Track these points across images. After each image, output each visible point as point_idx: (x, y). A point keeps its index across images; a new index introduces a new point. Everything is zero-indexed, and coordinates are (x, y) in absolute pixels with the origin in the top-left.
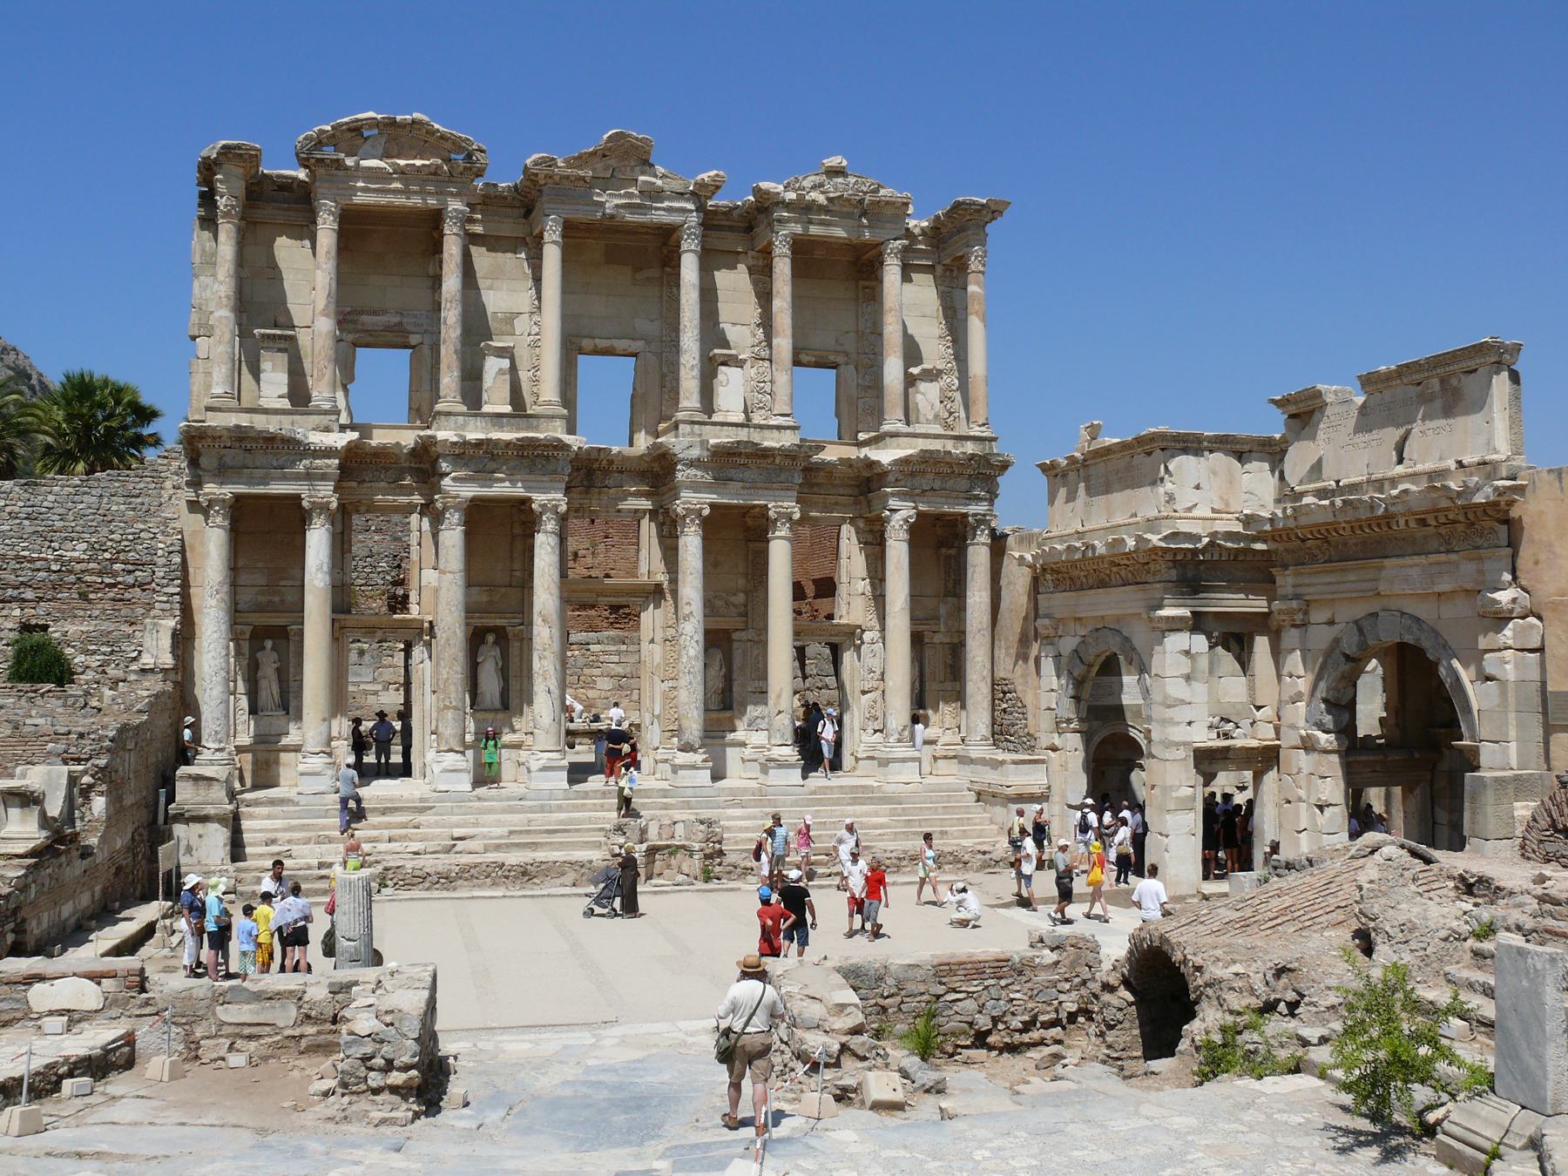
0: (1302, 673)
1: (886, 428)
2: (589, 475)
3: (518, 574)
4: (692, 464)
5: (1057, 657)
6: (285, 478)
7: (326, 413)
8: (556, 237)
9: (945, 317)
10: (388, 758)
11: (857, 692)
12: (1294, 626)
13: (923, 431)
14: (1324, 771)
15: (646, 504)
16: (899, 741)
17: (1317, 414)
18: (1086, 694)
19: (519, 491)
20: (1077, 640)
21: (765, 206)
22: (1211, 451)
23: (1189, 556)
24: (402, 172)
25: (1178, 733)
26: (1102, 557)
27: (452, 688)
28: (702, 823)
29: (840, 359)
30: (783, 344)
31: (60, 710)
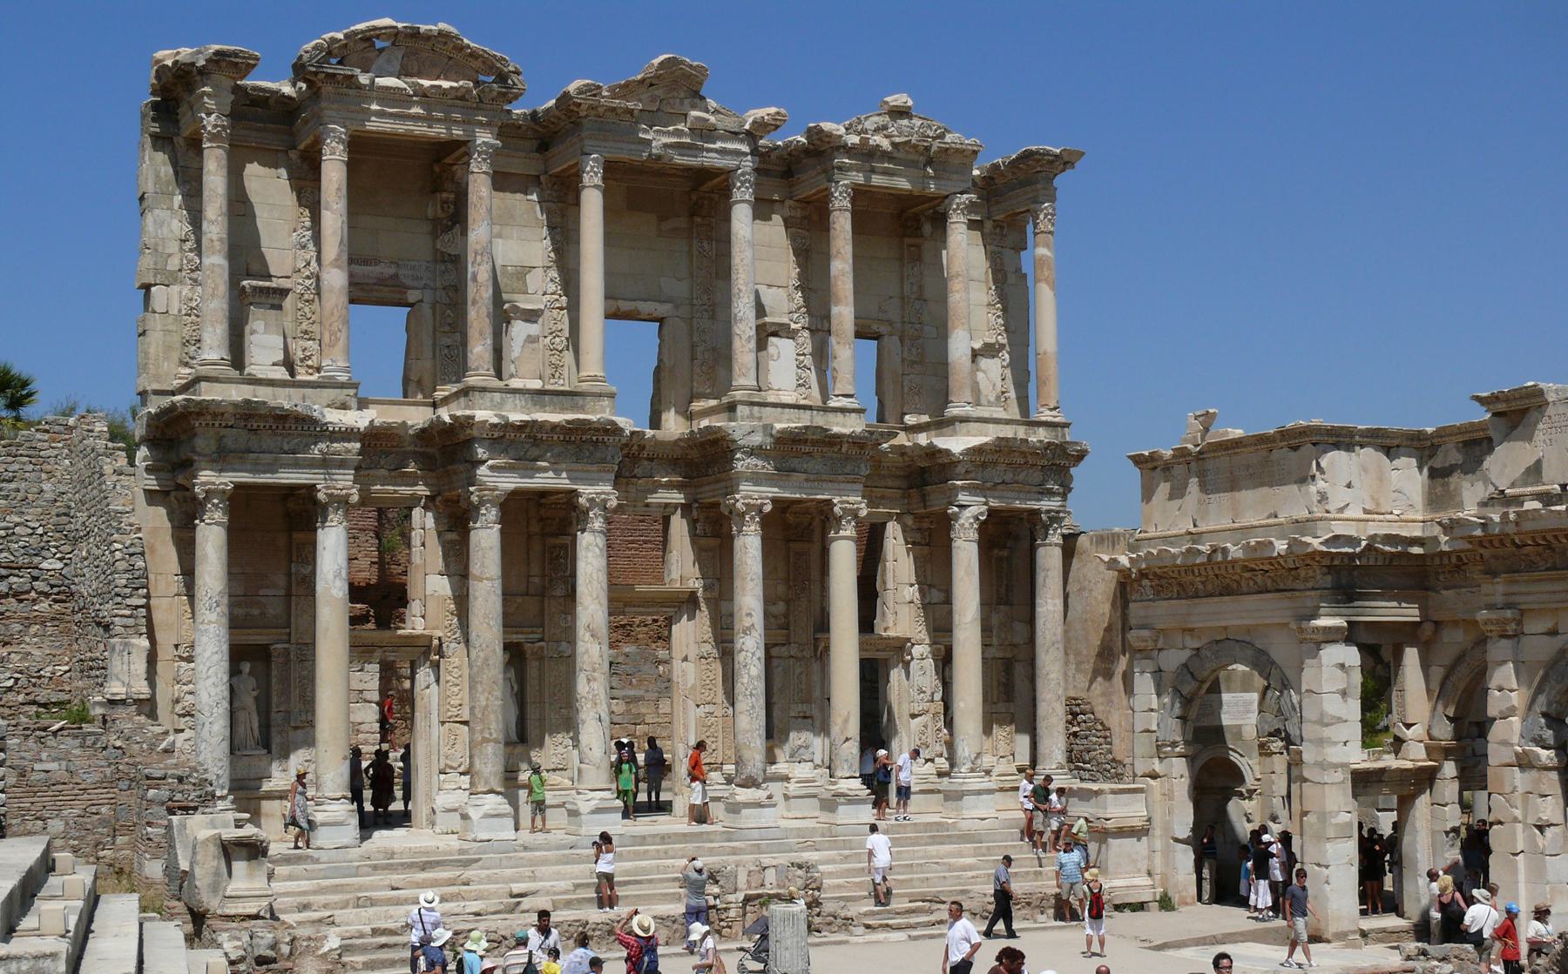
0: (1515, 686)
1: (953, 411)
2: (630, 460)
3: (536, 580)
4: (754, 452)
5: (1158, 673)
6: (297, 465)
7: (342, 386)
8: (598, 180)
9: (995, 281)
10: (658, 796)
11: (906, 716)
12: (1503, 636)
13: (986, 415)
14: (1545, 789)
15: (677, 497)
16: (972, 770)
17: (1534, 414)
18: (1193, 714)
19: (563, 482)
20: (1186, 654)
21: (821, 149)
22: (1362, 447)
23: (1346, 561)
24: (423, 94)
25: (1335, 754)
26: (1235, 561)
27: (492, 717)
28: (800, 867)
29: (883, 329)
30: (844, 313)
31: (77, 752)
